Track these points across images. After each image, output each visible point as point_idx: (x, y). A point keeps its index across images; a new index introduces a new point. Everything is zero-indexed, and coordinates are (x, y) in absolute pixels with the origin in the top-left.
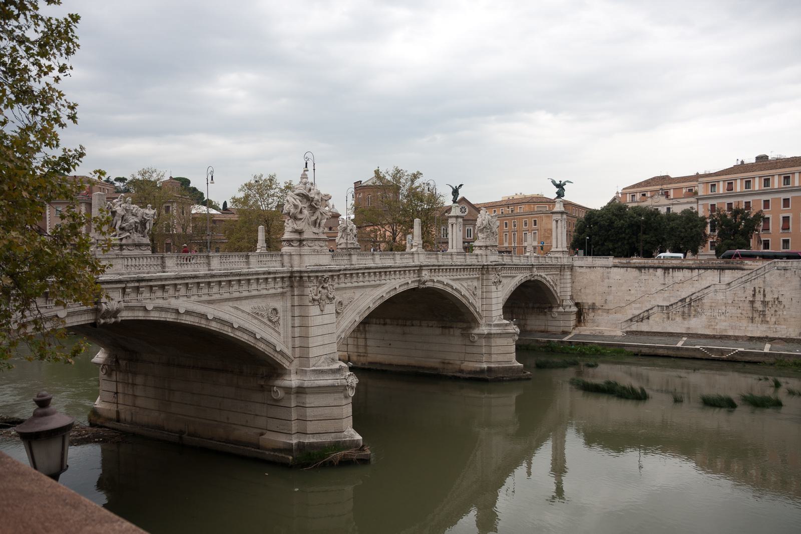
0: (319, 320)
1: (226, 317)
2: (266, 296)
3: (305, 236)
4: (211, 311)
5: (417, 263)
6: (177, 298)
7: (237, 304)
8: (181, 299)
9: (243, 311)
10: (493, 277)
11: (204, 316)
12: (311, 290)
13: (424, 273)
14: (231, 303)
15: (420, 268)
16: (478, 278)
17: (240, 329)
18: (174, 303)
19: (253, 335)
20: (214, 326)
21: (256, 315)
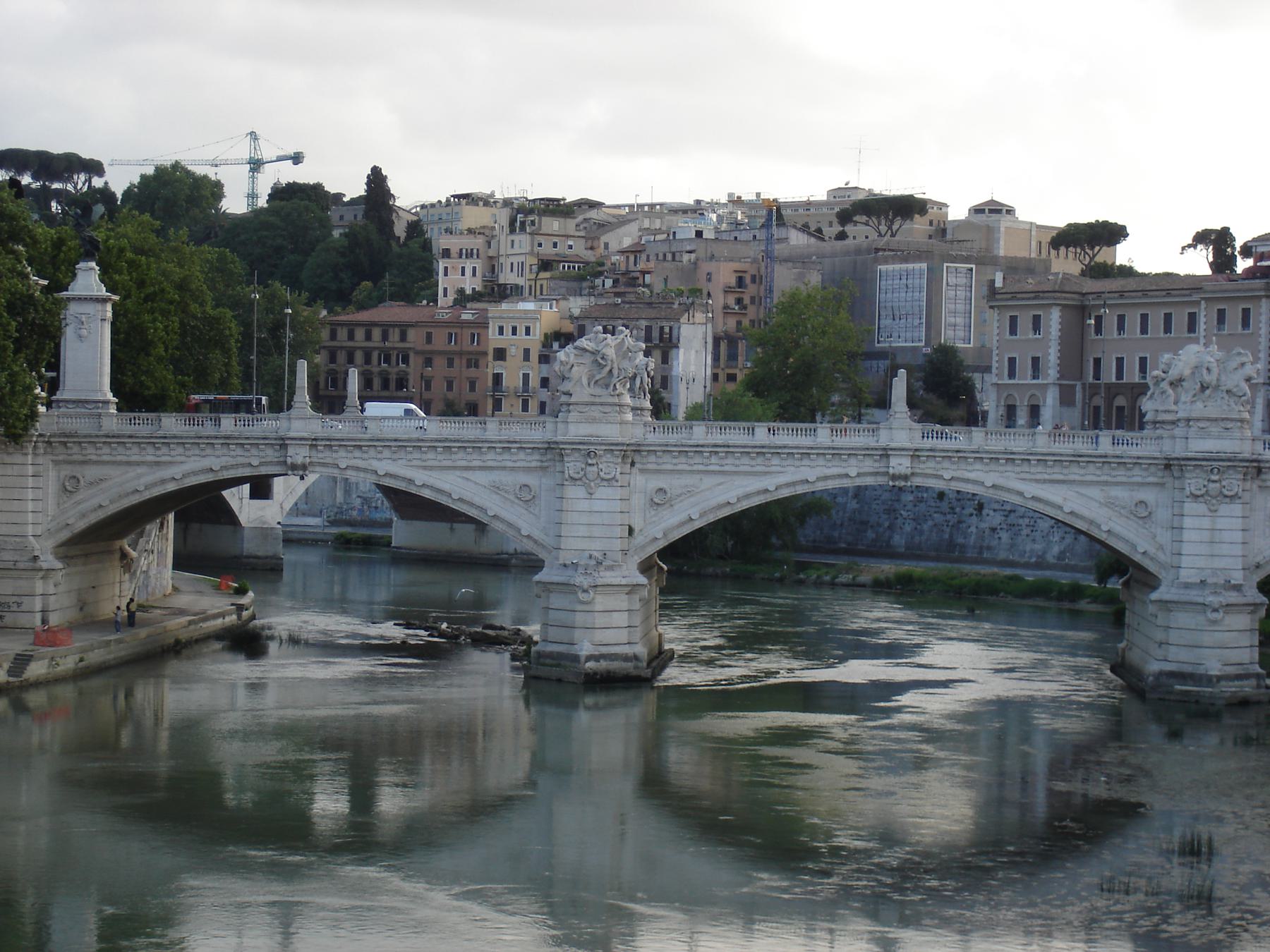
0: (584, 505)
1: (447, 487)
2: (512, 469)
3: (573, 400)
4: (420, 477)
5: (882, 443)
6: (380, 460)
7: (466, 474)
8: (384, 462)
9: (476, 483)
10: (1194, 482)
11: (410, 481)
12: (573, 465)
13: (894, 462)
14: (458, 473)
15: (885, 453)
16: (1162, 485)
17: (460, 500)
18: (375, 464)
19: (483, 510)
20: (427, 494)
21: (496, 488)
